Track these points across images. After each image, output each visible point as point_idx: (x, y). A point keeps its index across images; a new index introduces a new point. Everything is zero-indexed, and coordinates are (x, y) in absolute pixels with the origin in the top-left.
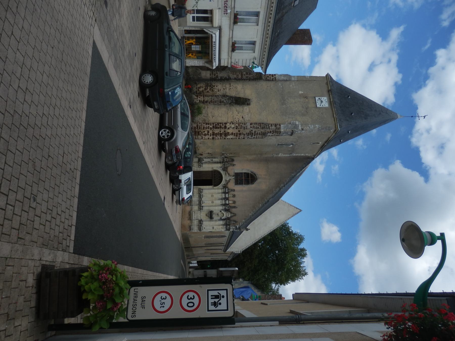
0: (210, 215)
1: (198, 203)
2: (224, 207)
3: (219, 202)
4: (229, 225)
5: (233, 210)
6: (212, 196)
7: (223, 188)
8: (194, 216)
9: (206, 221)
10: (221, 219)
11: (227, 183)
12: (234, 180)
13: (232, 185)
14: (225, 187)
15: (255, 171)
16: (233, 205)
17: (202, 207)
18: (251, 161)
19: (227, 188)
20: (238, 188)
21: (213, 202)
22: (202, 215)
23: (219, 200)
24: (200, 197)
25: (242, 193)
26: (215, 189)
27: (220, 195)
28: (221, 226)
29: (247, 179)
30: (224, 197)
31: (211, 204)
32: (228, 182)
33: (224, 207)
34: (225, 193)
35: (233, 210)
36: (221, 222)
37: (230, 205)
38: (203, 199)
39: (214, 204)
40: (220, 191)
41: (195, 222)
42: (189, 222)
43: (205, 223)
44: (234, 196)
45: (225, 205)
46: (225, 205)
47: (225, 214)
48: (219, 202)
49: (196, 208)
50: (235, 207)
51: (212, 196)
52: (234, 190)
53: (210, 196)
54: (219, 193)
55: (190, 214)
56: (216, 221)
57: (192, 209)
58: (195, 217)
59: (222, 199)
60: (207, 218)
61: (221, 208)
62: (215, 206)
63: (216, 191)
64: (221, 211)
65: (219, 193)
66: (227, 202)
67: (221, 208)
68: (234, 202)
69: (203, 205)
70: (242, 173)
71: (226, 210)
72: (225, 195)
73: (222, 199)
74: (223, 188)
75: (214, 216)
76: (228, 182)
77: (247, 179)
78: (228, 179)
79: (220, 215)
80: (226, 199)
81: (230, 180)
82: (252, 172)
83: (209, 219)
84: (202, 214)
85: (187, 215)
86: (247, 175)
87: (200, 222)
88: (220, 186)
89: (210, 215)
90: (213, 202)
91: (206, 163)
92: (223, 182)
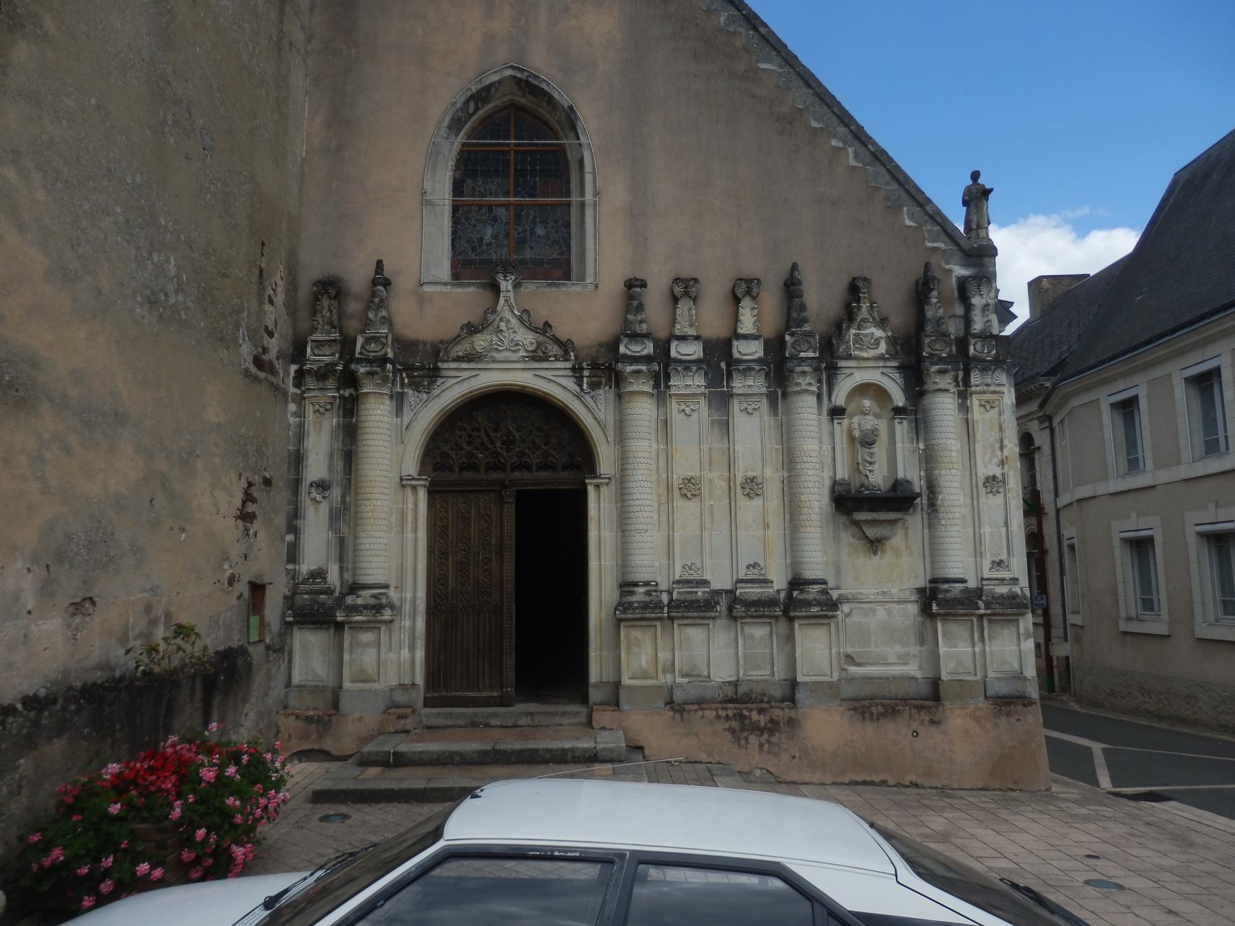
0: (869, 507)
1: (758, 632)
2: (805, 381)
3: (751, 428)
4: (963, 344)
5: (820, 300)
6: (691, 489)
7: (617, 380)
8: (895, 660)
9: (933, 550)
10: (914, 410)
11: (566, 347)
12: (530, 287)
13: (583, 310)
14: (603, 368)
15: (446, 93)
16: (771, 300)
17: (797, 583)
18: (341, 120)
19: (614, 345)
20: (606, 251)
21: (752, 487)
22: (878, 583)
23: (725, 427)
24: (693, 605)
25: (646, 215)
26: (623, 460)
27: (677, 418)
28: (977, 413)
29: (517, 164)
30: (697, 382)
31: (773, 497)
32: (550, 344)
33: (805, 381)
34: (663, 367)
35: (820, 300)
36: (944, 407)
37: (769, 329)
38: (721, 581)
39: (772, 475)
40: (643, 410)
41: (957, 651)
42: (957, 719)
43: (960, 564)
44: (684, 289)
45: (778, 369)
46: (778, 369)
47: (860, 377)
48: (751, 428)
49: (815, 651)
50: (791, 288)
51: (691, 489)
52: (634, 286)
53: (686, 510)
54: (665, 425)
55: (874, 704)
56: (929, 459)
57: (828, 690)
58: (893, 651)
59: (721, 400)
60: (897, 540)
61: (807, 411)
62: (789, 460)
63: (644, 447)
64: (837, 413)
65: (665, 425)
66: (751, 350)
67: (807, 411)
68: (743, 289)
69: (779, 581)
70: (456, 208)
71: (829, 363)
72: (687, 365)
73: (721, 400)
74: (617, 380)
75: (878, 477)
76: (550, 344)
77: (517, 164)
78: (527, 338)
79: (870, 422)
80: (719, 360)
81: (526, 319)
82: (456, 125)
83: (915, 522)
84: (868, 590)
85: (896, 734)
86: (472, 168)
87: (938, 601)
88: (592, 411)
89: (869, 507)
90: (752, 487)
91: (976, 393)
92: (555, 383)
